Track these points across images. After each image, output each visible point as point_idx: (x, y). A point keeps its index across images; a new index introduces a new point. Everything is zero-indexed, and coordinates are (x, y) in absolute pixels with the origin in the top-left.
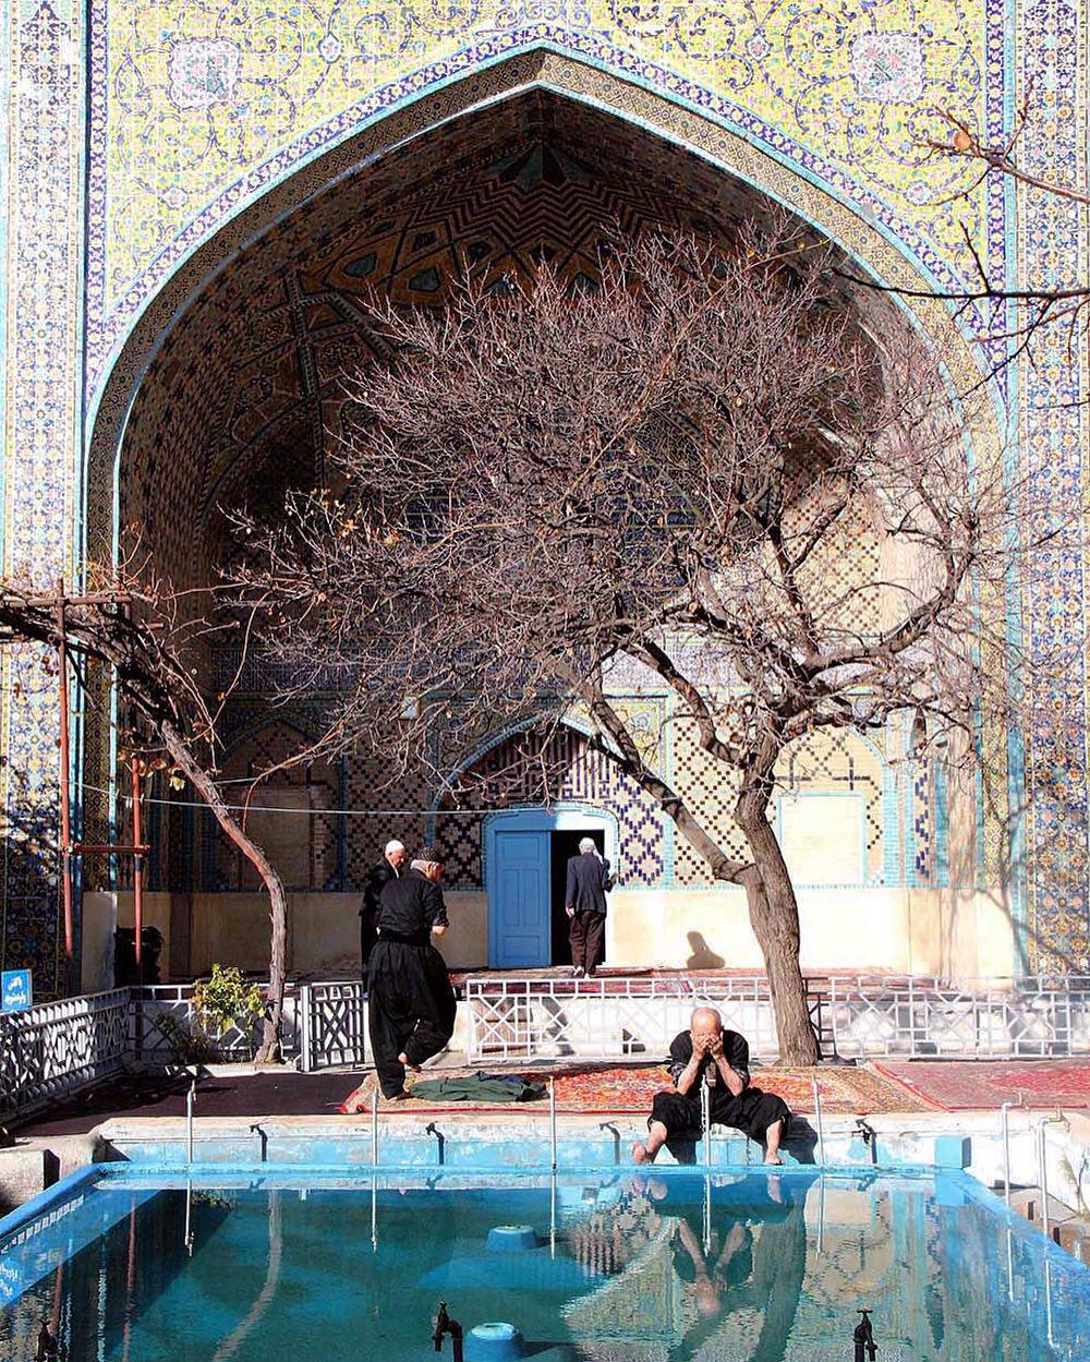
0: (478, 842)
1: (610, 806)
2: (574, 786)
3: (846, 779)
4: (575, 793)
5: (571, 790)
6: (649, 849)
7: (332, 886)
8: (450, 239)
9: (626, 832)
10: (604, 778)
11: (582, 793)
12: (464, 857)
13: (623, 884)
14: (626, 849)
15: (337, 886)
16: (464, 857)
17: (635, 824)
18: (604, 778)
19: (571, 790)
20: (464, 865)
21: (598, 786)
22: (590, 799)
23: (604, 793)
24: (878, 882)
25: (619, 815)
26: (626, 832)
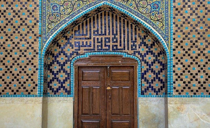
0: (69, 72)
1: (137, 54)
2: (118, 44)
4: (119, 47)
5: (116, 46)
6: (157, 76)
9: (145, 67)
10: (134, 40)
11: (122, 47)
12: (62, 79)
13: (143, 94)
14: (145, 76)
16: (62, 79)
17: (150, 63)
18: (134, 40)
19: (116, 46)
20: (62, 86)
21: (131, 43)
22: (126, 50)
23: (134, 47)
25: (141, 58)
26: (145, 67)
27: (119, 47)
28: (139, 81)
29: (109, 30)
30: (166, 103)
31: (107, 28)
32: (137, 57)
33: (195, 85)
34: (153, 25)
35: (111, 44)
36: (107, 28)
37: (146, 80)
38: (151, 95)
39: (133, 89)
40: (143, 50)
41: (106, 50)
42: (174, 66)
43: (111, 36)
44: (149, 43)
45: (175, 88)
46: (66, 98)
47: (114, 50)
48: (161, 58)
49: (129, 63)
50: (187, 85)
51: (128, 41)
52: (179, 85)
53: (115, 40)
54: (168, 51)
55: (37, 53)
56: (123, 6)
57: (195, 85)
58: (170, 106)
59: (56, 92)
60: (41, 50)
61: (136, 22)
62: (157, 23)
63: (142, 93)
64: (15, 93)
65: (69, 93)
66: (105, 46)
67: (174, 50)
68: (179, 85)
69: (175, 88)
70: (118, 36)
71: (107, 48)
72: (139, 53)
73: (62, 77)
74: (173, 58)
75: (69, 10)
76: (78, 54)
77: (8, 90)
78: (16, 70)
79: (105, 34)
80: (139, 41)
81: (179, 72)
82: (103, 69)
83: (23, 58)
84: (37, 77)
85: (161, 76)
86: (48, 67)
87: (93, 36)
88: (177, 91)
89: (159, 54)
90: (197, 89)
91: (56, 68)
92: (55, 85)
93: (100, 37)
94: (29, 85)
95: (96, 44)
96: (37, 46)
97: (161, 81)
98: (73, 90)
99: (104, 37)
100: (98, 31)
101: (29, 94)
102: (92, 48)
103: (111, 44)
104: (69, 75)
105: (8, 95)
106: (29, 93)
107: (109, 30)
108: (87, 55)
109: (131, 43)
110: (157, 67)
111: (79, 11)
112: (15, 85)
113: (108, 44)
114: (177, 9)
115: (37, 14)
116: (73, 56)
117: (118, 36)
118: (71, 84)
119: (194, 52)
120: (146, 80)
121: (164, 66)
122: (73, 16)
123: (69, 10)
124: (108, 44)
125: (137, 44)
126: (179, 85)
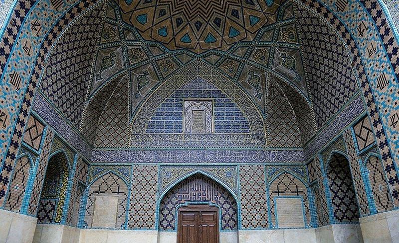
3: (296, 192)
4: (207, 199)
7: (123, 228)
8: (171, 15)
15: (124, 228)
21: (214, 196)
24: (310, 227)
27: (207, 199)
28: (220, 221)
29: (201, 188)
30: (238, 234)
31: (199, 187)
32: (219, 205)
33: (255, 222)
34: (228, 185)
35: (202, 197)
36: (199, 187)
39: (216, 226)
40: (222, 201)
41: (199, 201)
42: (242, 210)
43: (202, 192)
45: (243, 224)
46: (172, 232)
49: (214, 209)
50: (250, 223)
51: (213, 196)
52: (245, 222)
53: (204, 194)
54: (237, 201)
55: (155, 202)
56: (209, 173)
57: (255, 222)
58: (240, 236)
59: (165, 228)
61: (218, 183)
62: (230, 183)
63: (222, 229)
64: (141, 227)
65: (174, 229)
66: (198, 198)
67: (241, 200)
68: (245, 222)
69: (243, 224)
70: (206, 192)
71: (199, 199)
73: (169, 218)
74: (241, 205)
75: (176, 176)
76: (180, 203)
78: (141, 212)
79: (198, 191)
80: (220, 195)
81: (245, 214)
82: (197, 213)
84: (155, 217)
85: (234, 218)
86: (161, 211)
87: (190, 192)
88: (244, 226)
90: (256, 224)
91: (166, 212)
92: (165, 223)
95: (192, 197)
96: (155, 197)
98: (177, 228)
99: (197, 192)
100: (193, 188)
101: (149, 228)
102: (190, 199)
103: (202, 197)
104: (174, 216)
105: (136, 229)
106: (150, 228)
107: (201, 188)
108: (186, 204)
109: (214, 196)
110: (231, 212)
112: (141, 222)
113: (199, 197)
114: (241, 176)
115: (157, 178)
116: (177, 204)
117: (206, 192)
118: (175, 223)
119: (253, 202)
121: (236, 211)
123: (176, 176)
124: (199, 197)
125: (219, 197)
126: (245, 222)
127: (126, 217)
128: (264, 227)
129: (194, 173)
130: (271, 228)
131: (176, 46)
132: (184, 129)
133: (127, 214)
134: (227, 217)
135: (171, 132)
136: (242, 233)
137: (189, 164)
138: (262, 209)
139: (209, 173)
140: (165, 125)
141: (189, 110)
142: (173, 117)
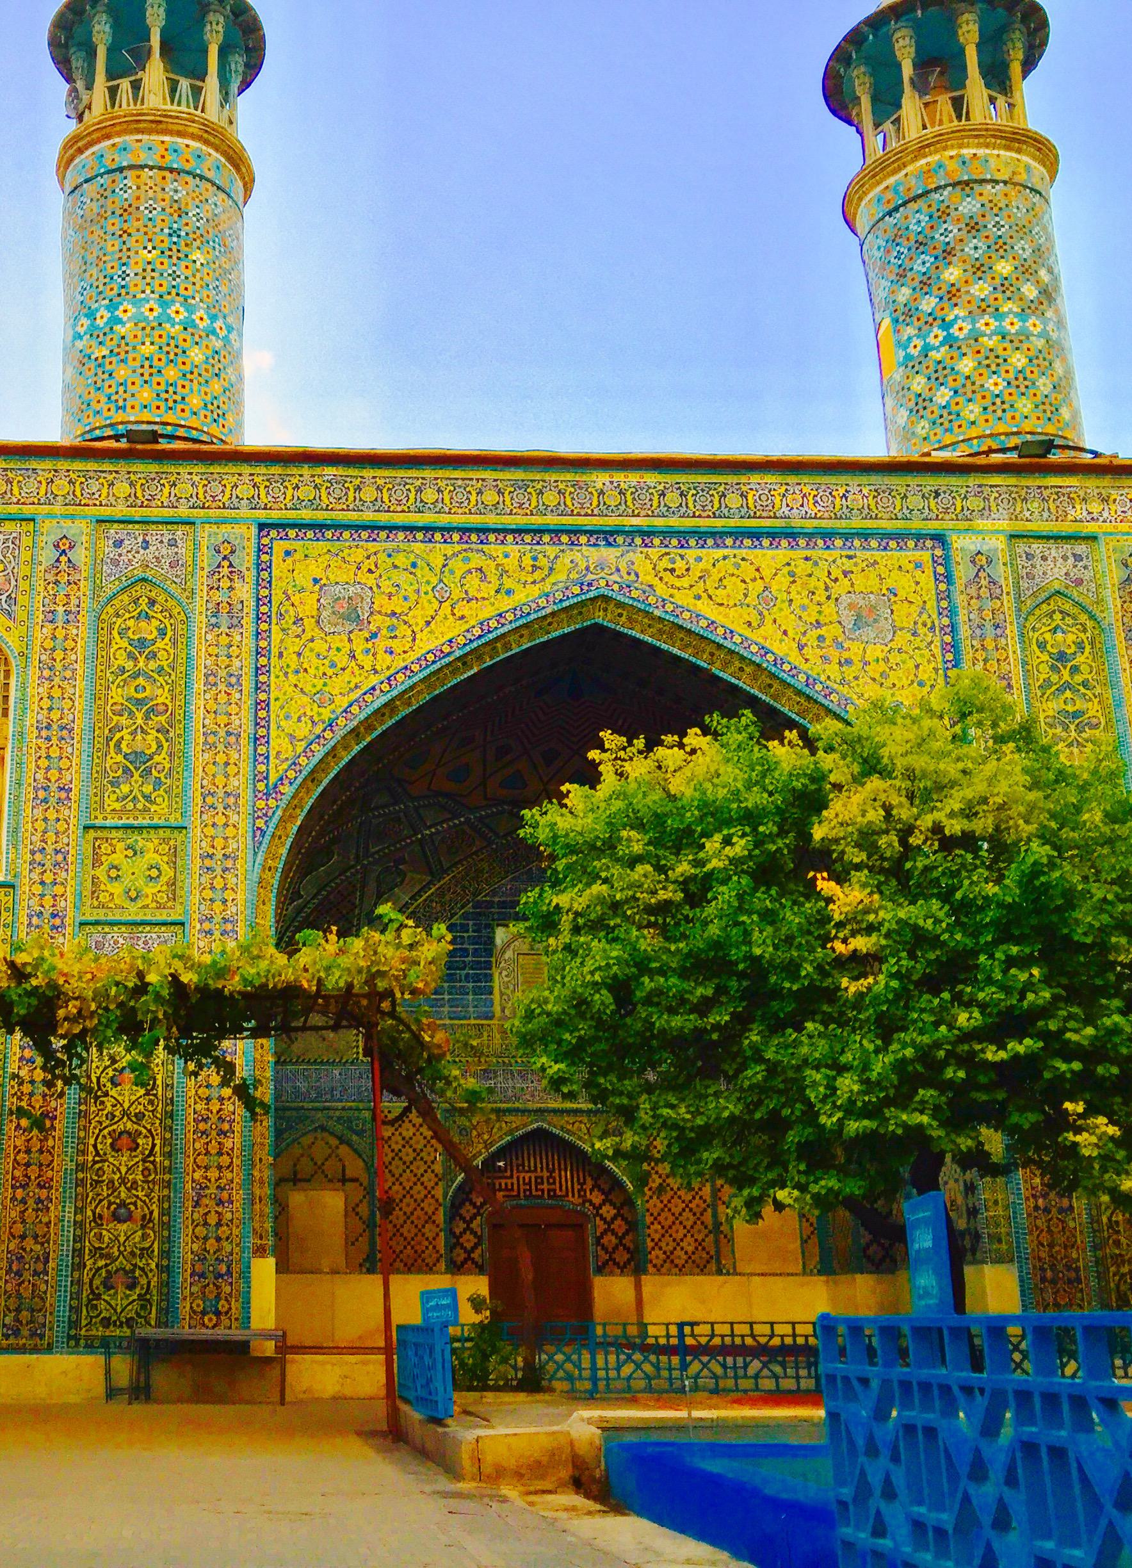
9: (602, 1226)
12: (468, 1246)
16: (468, 1246)
21: (577, 1187)
26: (602, 1226)
37: (604, 1248)
38: (611, 1273)
40: (597, 1198)
44: (606, 1187)
47: (550, 1197)
48: (625, 1211)
56: (568, 1132)
60: (445, 1197)
70: (556, 1174)
72: (590, 1201)
77: (398, 1264)
80: (589, 1183)
83: (418, 1212)
85: (627, 1241)
89: (622, 1205)
93: (527, 1176)
94: (429, 1256)
96: (439, 1193)
97: (628, 1249)
104: (480, 1238)
109: (577, 1187)
111: (501, 1138)
120: (604, 1248)
121: (633, 1226)
122: (492, 1145)
127: (372, 1244)
128: (702, 1270)
129: (529, 1128)
130: (719, 1272)
131: (486, 798)
132: (497, 1009)
133: (372, 1237)
134: (610, 1240)
135: (465, 1018)
136: (649, 1283)
137: (517, 1105)
138: (699, 1226)
139: (568, 1132)
140: (447, 997)
141: (509, 954)
142: (467, 975)
